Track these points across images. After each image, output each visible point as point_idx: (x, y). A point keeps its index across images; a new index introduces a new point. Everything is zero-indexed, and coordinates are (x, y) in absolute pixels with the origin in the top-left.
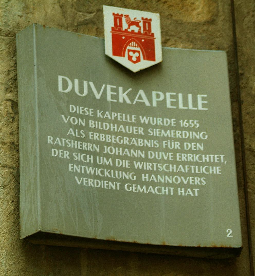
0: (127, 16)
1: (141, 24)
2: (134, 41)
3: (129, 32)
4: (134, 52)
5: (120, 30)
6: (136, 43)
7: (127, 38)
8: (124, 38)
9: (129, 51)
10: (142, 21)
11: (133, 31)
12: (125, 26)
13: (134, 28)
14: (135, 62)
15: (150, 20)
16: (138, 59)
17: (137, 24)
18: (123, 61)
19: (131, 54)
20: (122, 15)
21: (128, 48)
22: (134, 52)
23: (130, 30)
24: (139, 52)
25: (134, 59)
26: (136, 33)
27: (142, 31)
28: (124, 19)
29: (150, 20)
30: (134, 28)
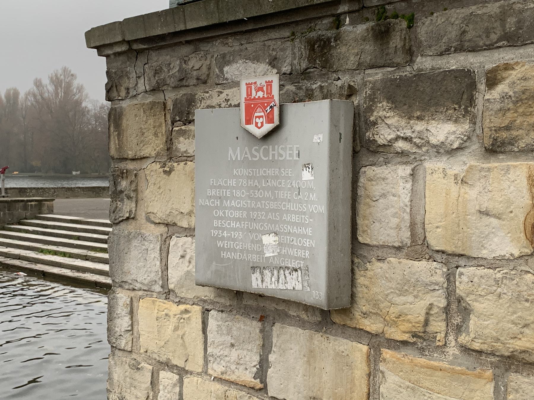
0: (255, 83)
1: (265, 88)
2: (259, 107)
3: (257, 99)
4: (259, 117)
5: (250, 99)
6: (261, 108)
7: (255, 105)
8: (252, 106)
9: (256, 117)
10: (265, 85)
11: (259, 97)
12: (254, 92)
13: (260, 94)
14: (259, 128)
15: (272, 81)
16: (262, 125)
17: (261, 89)
18: (251, 128)
19: (257, 119)
20: (252, 84)
21: (256, 114)
22: (259, 117)
23: (257, 97)
24: (262, 117)
25: (259, 125)
26: (261, 99)
27: (265, 96)
28: (253, 87)
29: (272, 81)
30: (260, 94)
